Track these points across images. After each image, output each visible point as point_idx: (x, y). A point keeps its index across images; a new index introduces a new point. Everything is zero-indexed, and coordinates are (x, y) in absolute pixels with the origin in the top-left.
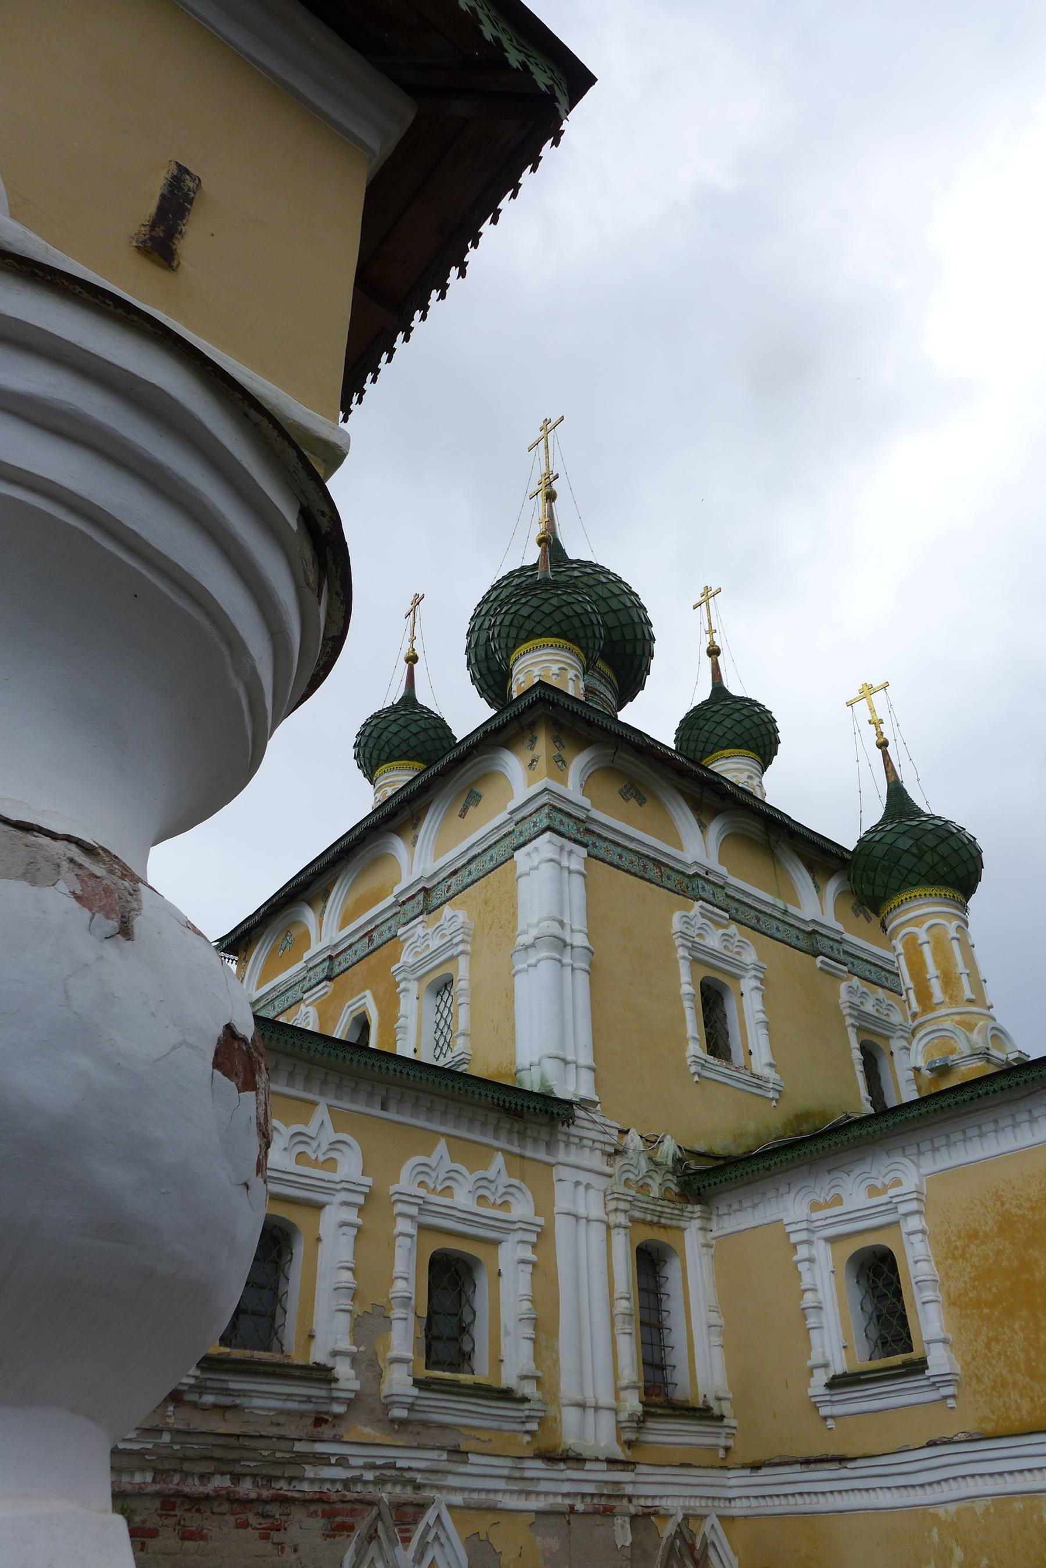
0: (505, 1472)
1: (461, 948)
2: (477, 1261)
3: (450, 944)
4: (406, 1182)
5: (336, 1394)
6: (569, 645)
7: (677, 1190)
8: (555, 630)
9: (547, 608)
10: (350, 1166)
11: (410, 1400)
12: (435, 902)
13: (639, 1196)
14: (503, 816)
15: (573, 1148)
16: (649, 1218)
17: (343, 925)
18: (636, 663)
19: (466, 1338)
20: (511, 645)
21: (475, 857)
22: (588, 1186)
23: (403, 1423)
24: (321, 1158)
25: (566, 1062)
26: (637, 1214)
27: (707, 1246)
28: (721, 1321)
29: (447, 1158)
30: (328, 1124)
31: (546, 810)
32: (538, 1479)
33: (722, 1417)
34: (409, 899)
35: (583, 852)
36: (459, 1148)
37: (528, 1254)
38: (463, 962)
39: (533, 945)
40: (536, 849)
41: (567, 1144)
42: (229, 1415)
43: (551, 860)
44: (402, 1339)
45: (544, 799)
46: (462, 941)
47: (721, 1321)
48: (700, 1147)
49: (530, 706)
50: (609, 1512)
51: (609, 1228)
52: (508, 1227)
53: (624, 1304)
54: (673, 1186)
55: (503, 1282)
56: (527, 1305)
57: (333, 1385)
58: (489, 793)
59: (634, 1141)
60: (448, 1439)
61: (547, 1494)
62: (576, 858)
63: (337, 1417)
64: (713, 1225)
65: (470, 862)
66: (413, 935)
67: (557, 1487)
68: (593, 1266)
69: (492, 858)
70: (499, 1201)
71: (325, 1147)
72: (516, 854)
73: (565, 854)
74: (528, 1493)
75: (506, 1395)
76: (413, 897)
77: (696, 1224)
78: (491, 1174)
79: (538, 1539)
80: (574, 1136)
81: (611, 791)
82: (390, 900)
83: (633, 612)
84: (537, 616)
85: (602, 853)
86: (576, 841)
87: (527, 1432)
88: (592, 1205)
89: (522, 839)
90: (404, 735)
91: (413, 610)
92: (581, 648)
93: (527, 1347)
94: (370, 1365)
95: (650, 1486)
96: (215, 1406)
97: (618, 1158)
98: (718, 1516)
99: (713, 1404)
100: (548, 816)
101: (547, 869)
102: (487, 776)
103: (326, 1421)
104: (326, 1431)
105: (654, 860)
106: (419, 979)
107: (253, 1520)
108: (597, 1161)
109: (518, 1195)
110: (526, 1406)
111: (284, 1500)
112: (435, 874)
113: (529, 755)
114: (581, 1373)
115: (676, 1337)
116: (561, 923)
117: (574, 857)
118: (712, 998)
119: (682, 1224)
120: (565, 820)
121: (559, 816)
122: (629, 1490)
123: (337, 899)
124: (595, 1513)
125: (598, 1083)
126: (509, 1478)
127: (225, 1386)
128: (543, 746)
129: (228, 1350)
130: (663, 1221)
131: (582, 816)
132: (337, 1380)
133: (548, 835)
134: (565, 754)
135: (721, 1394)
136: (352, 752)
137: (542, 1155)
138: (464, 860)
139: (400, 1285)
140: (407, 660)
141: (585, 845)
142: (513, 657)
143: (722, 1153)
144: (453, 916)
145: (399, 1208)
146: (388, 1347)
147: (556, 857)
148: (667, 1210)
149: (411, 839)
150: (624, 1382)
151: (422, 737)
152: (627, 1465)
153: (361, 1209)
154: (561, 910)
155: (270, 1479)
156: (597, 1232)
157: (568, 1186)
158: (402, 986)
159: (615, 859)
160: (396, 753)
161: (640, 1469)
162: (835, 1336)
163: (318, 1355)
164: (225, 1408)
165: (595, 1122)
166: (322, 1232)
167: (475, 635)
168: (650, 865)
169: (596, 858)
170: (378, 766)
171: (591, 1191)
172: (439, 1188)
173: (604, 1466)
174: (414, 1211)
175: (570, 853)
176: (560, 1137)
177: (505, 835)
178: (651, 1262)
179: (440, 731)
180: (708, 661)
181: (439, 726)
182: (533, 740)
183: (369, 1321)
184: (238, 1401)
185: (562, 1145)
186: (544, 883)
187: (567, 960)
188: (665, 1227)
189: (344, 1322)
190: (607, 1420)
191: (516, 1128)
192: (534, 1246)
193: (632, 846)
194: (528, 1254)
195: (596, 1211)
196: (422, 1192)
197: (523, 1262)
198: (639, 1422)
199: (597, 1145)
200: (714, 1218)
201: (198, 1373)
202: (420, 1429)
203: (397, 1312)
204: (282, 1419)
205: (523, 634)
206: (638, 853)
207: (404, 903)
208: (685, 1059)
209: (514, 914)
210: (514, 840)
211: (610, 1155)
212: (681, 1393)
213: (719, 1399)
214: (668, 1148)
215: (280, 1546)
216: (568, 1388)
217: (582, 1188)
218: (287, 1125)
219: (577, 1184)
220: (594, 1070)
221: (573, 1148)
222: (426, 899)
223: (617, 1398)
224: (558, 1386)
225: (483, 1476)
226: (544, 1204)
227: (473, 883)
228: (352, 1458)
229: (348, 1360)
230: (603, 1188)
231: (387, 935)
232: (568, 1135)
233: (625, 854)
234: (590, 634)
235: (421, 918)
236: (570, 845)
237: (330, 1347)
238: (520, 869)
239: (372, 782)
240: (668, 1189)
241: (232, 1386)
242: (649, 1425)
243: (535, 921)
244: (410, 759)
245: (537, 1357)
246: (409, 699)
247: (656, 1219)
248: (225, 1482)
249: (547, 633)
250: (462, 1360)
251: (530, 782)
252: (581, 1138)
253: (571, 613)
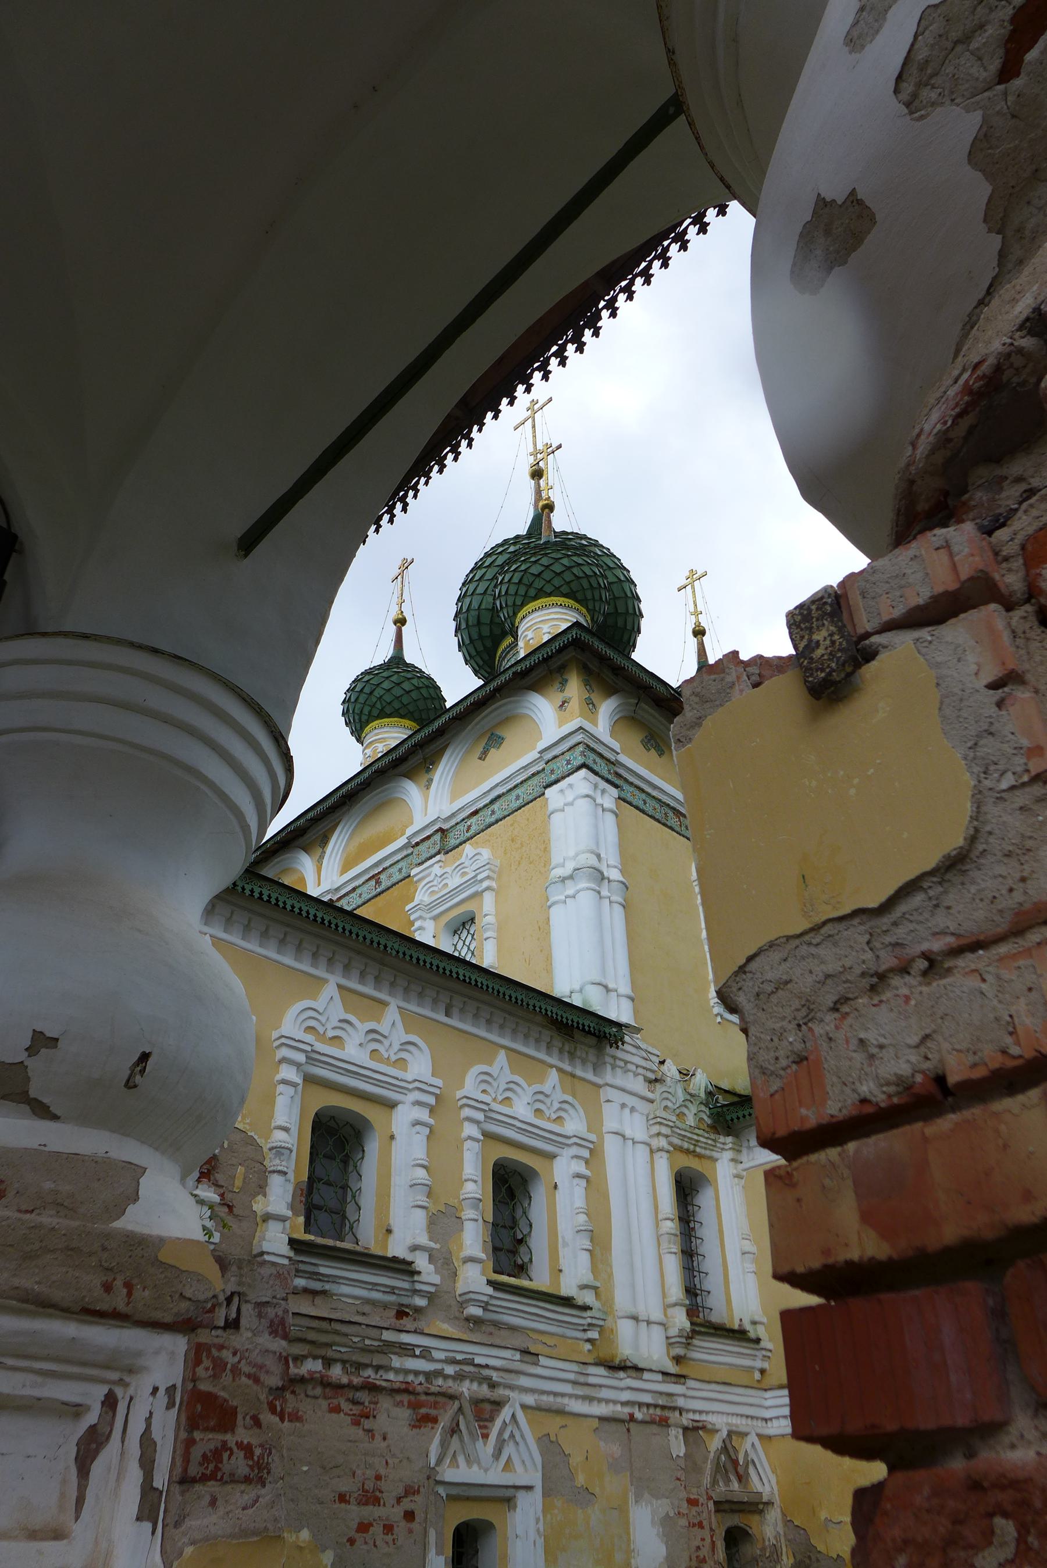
0: (571, 1376)
1: (485, 884)
2: (533, 1173)
3: (474, 880)
4: (470, 1086)
5: (418, 1286)
6: (577, 605)
7: (709, 1121)
8: (565, 589)
9: (557, 568)
10: (420, 1066)
11: (485, 1299)
12: (453, 842)
13: (678, 1123)
14: (534, 755)
15: (619, 1070)
16: (686, 1145)
17: (344, 870)
18: (626, 637)
19: (522, 1249)
20: (518, 602)
21: (499, 797)
22: (633, 1110)
23: (477, 1321)
24: (393, 1058)
25: (607, 989)
26: (676, 1141)
27: (738, 1176)
28: (754, 1249)
29: (507, 1070)
30: (399, 1025)
31: (581, 748)
32: (601, 1386)
33: (758, 1341)
34: (423, 840)
35: (615, 792)
37: (581, 1168)
38: (488, 899)
39: (571, 877)
40: (571, 786)
41: (614, 1067)
42: (318, 1300)
43: (587, 796)
44: (473, 1240)
45: (579, 737)
46: (488, 877)
47: (754, 1249)
48: (725, 1086)
49: (560, 650)
50: (664, 1423)
51: (652, 1152)
52: (563, 1141)
53: (669, 1224)
54: (705, 1118)
55: (560, 1196)
56: (582, 1218)
57: (416, 1278)
58: (512, 736)
59: (671, 1070)
60: (519, 1341)
61: (607, 1401)
62: (609, 798)
63: (418, 1310)
64: (744, 1157)
65: (492, 802)
66: (429, 875)
67: (618, 1394)
68: (640, 1185)
69: (518, 797)
70: (554, 1116)
71: (396, 1046)
72: (547, 791)
73: (599, 792)
74: (590, 1399)
75: (567, 1302)
76: (428, 838)
77: (728, 1155)
78: (547, 1088)
79: (602, 1444)
80: (620, 1059)
81: (635, 739)
82: (402, 841)
83: (626, 586)
84: (547, 575)
85: (630, 798)
86: (608, 781)
87: (589, 1340)
88: (636, 1127)
89: (553, 777)
90: (397, 691)
91: (401, 574)
92: (588, 610)
93: (584, 1258)
94: (445, 1261)
95: (698, 1401)
96: (306, 1291)
97: (658, 1085)
98: (758, 1435)
99: (748, 1327)
100: (583, 754)
101: (584, 805)
102: (509, 720)
103: (407, 1314)
104: (407, 1323)
105: (673, 809)
106: (435, 918)
107: (345, 1406)
108: (639, 1085)
109: (571, 1111)
110: (589, 1313)
111: (372, 1388)
112: (453, 815)
113: (559, 698)
114: (633, 1286)
115: (710, 1263)
116: (598, 856)
117: (606, 795)
119: (715, 1154)
120: (598, 760)
121: (592, 756)
122: (681, 1402)
123: (337, 845)
124: (652, 1422)
125: (636, 1012)
126: (575, 1383)
127: (316, 1270)
128: (574, 688)
129: (312, 1238)
130: (698, 1150)
131: (612, 758)
132: (419, 1273)
133: (583, 772)
134: (595, 697)
135: (757, 1318)
136: (340, 709)
137: (590, 1076)
138: (486, 800)
139: (470, 1187)
140: (395, 623)
141: (616, 786)
142: (520, 615)
143: (742, 1093)
144: (476, 856)
145: (467, 1112)
146: (461, 1247)
147: (591, 793)
148: (702, 1139)
149: (424, 782)
150: (672, 1299)
151: (414, 695)
152: (680, 1378)
153: (432, 1110)
154: (597, 844)
155: (360, 1366)
156: (642, 1152)
157: (615, 1106)
158: (417, 924)
160: (388, 710)
161: (691, 1383)
163: (397, 1249)
164: (314, 1293)
165: (638, 1048)
166: (395, 1129)
167: (467, 600)
168: (671, 814)
169: (624, 800)
170: (368, 722)
171: (635, 1114)
172: (500, 1098)
173: (660, 1377)
174: (480, 1116)
175: (603, 791)
176: (608, 1059)
177: (533, 775)
178: (687, 1188)
179: (431, 691)
180: (693, 642)
181: (430, 689)
182: (564, 683)
183: (443, 1220)
184: (327, 1287)
185: (609, 1067)
186: (578, 819)
187: (605, 892)
188: (700, 1156)
189: (420, 1217)
191: (567, 1048)
192: (587, 1162)
193: (654, 793)
195: (640, 1135)
196: (487, 1099)
197: (578, 1176)
198: (688, 1338)
199: (640, 1070)
200: (745, 1151)
201: (291, 1254)
202: (491, 1329)
203: (468, 1213)
204: (367, 1309)
205: (532, 592)
206: (660, 800)
207: (417, 844)
208: (708, 1001)
209: (546, 850)
210: (547, 775)
211: (650, 1082)
212: (716, 1317)
213: (754, 1323)
214: (700, 1082)
215: (369, 1431)
216: (622, 1301)
217: (627, 1111)
218: (362, 1021)
219: (623, 1106)
220: (632, 999)
221: (619, 1070)
222: (443, 839)
223: (665, 1315)
224: (613, 1299)
225: (552, 1378)
226: (595, 1121)
227: (497, 821)
228: (434, 1351)
229: (426, 1255)
230: (646, 1112)
231: (397, 877)
232: (615, 1058)
233: (648, 800)
234: (597, 597)
235: (438, 858)
236: (603, 784)
237: (409, 1241)
238: (552, 806)
239: (359, 740)
240: (701, 1119)
241: (323, 1270)
242: (695, 1342)
243: (572, 853)
244: (402, 717)
245: (594, 1269)
246: (397, 659)
247: (692, 1147)
248: (313, 1366)
249: (556, 592)
250: (521, 1270)
251: (561, 723)
252: (626, 1062)
253: (581, 575)
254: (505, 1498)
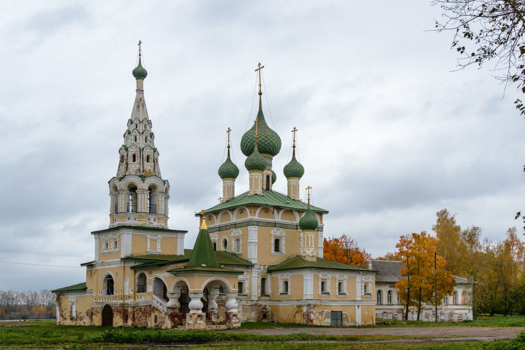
59: (262, 267)
67: (250, 303)
95: (260, 303)
108: (257, 270)
115: (266, 288)
118: (277, 242)
159: (262, 225)
162: (281, 290)
178: (263, 280)
190: (257, 297)
216: (253, 294)
226: (251, 277)
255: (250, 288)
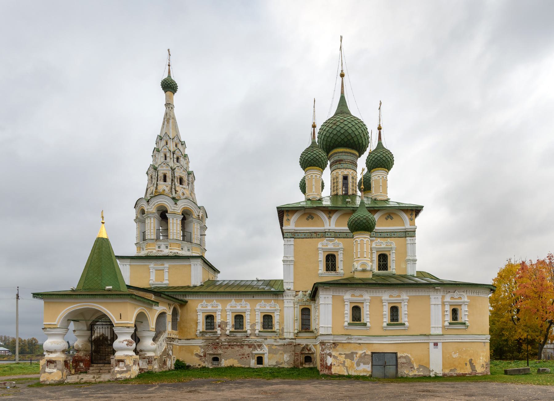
36: (265, 300)
67: (281, 342)
95: (298, 341)
152: (295, 339)
156: (293, 308)
159: (303, 236)
183: (253, 325)
189: (249, 326)
194: (278, 313)
225: (270, 341)
254: (264, 354)
255: (281, 323)
